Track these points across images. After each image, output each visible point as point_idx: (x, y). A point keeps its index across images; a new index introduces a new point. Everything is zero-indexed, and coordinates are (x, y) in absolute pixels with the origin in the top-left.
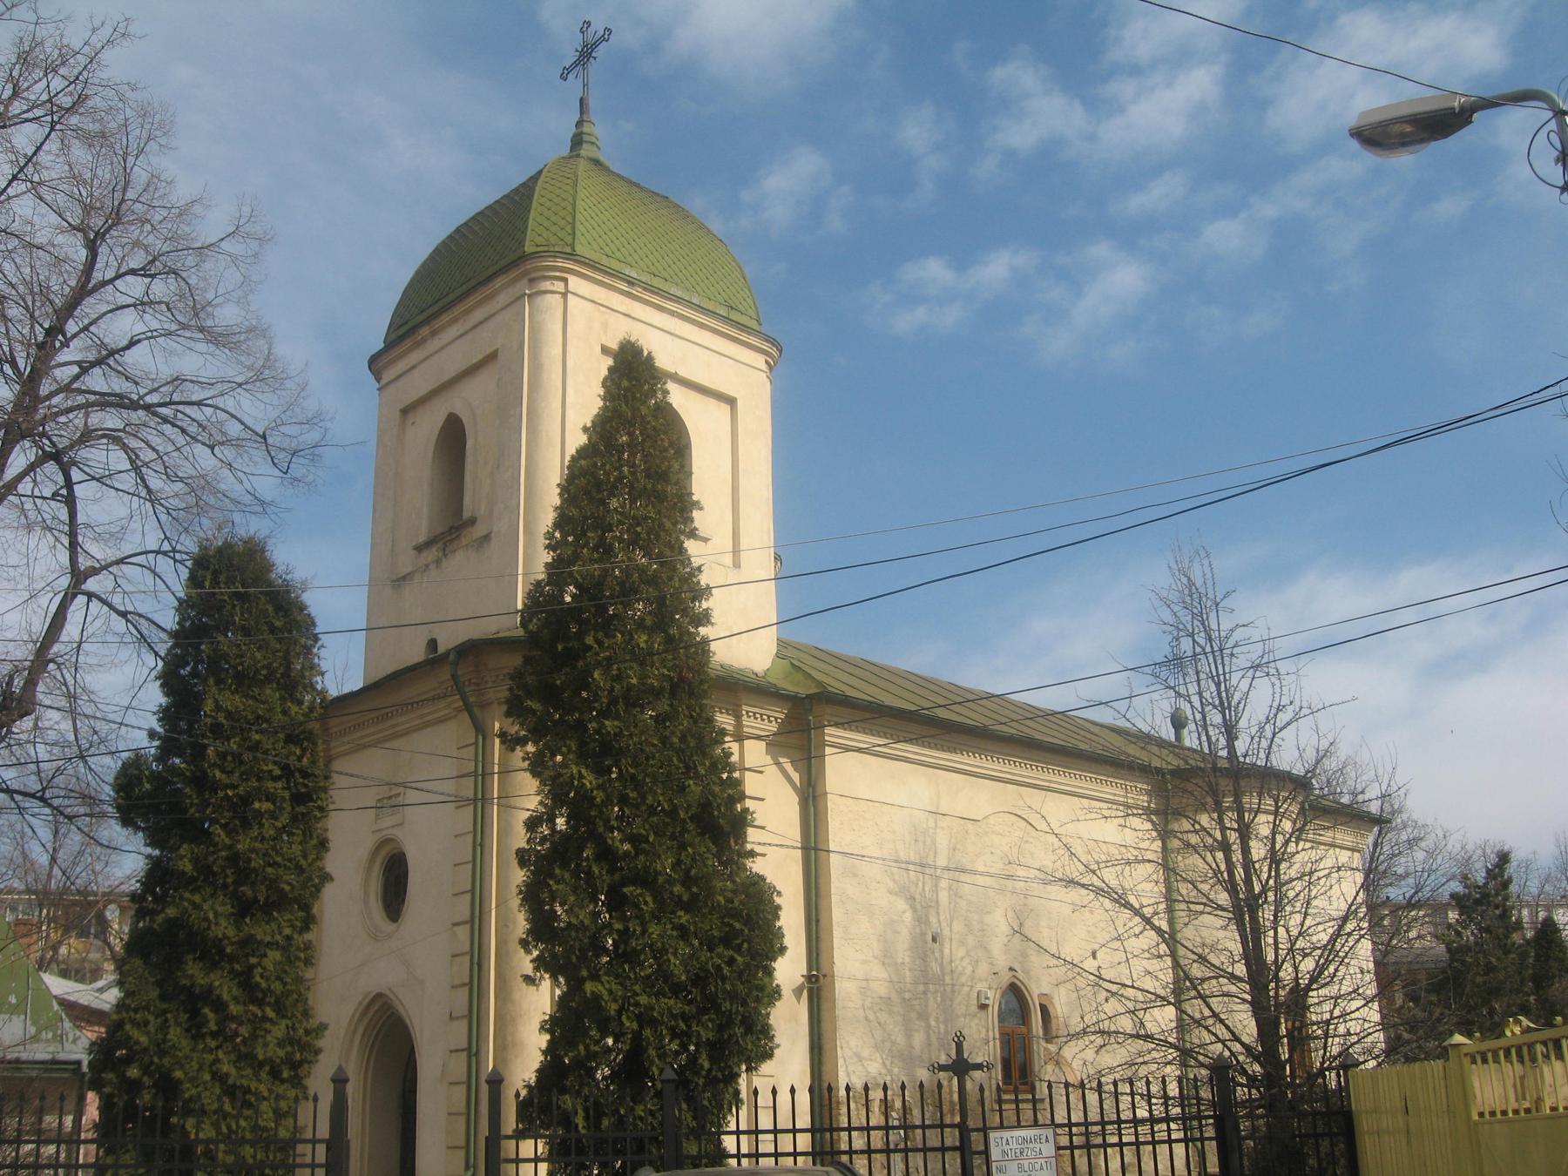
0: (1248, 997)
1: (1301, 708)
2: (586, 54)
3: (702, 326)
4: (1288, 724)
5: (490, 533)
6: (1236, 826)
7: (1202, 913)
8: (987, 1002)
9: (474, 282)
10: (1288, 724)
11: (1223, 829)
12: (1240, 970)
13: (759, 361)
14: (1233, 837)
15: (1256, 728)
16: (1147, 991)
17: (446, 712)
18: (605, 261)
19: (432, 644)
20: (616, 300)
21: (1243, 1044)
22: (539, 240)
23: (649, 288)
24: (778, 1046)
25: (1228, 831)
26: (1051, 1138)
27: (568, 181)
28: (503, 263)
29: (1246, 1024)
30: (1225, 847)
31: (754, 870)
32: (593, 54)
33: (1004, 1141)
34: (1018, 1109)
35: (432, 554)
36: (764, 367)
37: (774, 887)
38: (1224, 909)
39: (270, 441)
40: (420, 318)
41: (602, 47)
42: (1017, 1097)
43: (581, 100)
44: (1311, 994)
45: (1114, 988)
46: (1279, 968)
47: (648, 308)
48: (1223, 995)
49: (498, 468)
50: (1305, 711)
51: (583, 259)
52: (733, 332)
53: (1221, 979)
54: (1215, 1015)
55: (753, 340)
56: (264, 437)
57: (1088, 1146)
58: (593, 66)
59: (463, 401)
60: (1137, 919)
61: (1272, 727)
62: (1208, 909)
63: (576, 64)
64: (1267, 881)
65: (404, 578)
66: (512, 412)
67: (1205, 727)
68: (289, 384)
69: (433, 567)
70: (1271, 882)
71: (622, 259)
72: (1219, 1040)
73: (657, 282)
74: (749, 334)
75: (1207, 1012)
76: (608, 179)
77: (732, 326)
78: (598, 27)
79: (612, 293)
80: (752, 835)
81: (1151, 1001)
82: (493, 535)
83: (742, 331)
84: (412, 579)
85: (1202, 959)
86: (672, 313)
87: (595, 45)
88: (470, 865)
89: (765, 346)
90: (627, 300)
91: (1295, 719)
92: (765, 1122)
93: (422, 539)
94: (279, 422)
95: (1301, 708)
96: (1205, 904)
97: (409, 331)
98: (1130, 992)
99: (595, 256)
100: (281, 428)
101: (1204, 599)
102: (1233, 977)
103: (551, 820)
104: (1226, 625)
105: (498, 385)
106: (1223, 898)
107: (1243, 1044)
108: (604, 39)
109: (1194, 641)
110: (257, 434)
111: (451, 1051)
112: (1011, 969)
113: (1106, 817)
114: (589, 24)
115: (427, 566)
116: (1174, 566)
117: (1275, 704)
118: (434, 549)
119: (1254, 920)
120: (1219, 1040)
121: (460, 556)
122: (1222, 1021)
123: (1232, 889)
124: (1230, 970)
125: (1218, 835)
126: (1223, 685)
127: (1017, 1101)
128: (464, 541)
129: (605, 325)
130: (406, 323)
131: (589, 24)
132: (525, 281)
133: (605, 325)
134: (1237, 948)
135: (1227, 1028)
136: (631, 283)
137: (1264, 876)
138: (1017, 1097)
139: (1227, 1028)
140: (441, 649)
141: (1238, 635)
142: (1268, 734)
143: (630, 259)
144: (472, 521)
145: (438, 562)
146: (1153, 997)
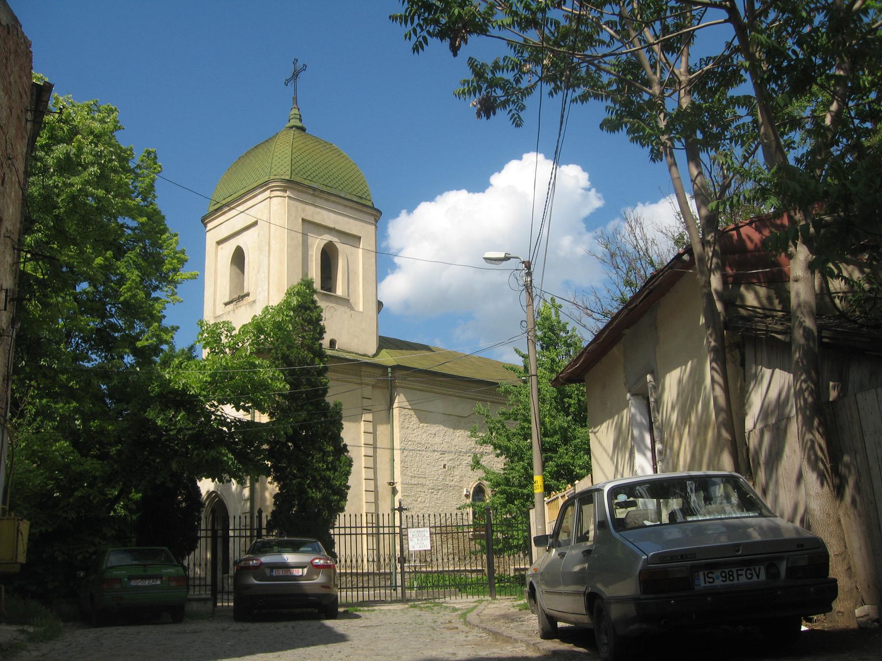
2: (295, 75)
3: (346, 206)
9: (247, 189)
22: (275, 173)
35: (231, 307)
40: (224, 202)
41: (303, 73)
43: (294, 98)
49: (259, 272)
52: (360, 207)
55: (369, 210)
59: (245, 241)
65: (219, 316)
69: (232, 312)
73: (324, 189)
76: (304, 141)
78: (300, 65)
87: (299, 72)
89: (374, 212)
93: (227, 300)
99: (298, 179)
115: (229, 312)
121: (243, 308)
129: (304, 210)
133: (304, 210)
143: (315, 180)
144: (248, 295)
145: (234, 310)
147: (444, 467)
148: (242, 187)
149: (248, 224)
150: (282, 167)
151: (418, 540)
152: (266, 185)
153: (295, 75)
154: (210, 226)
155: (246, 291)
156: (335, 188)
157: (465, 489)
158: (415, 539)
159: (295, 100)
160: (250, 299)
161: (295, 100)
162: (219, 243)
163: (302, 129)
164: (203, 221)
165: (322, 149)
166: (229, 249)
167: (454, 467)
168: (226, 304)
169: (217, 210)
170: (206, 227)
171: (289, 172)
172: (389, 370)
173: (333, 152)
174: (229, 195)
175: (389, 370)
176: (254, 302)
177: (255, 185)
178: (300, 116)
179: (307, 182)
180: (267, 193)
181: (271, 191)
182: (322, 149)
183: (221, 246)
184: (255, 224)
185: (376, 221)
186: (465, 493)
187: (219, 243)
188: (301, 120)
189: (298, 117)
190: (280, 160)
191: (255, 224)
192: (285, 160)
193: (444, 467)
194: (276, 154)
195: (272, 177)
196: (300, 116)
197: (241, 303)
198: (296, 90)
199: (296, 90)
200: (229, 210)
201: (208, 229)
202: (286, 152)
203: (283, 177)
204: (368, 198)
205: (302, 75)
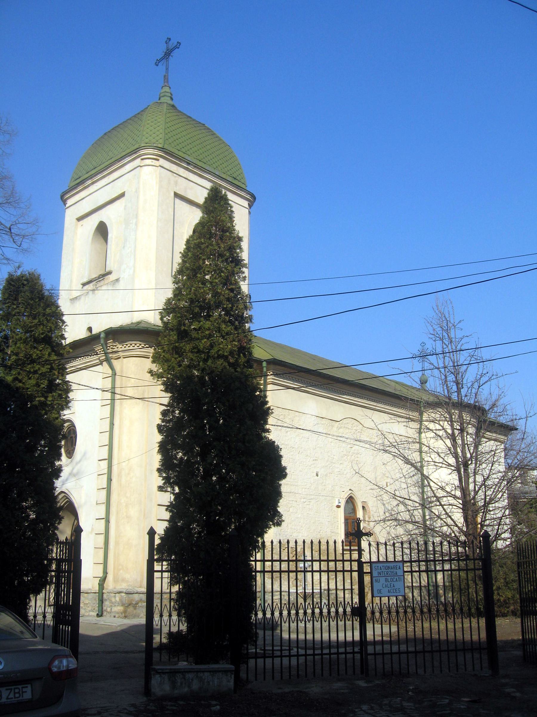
0: (461, 506)
1: (493, 375)
2: (168, 54)
4: (486, 382)
5: (119, 278)
6: (458, 427)
7: (441, 467)
8: (340, 504)
10: (486, 382)
11: (453, 429)
12: (458, 493)
13: (246, 204)
14: (456, 432)
15: (471, 384)
16: (416, 502)
17: (98, 361)
18: (177, 152)
19: (90, 329)
20: (182, 171)
21: (459, 528)
22: (147, 140)
23: (196, 166)
24: (284, 521)
25: (455, 430)
26: (401, 567)
27: (160, 113)
28: (128, 151)
29: (458, 517)
30: (453, 438)
31: (270, 439)
32: (171, 54)
33: (379, 568)
34: (351, 554)
35: (90, 287)
36: (247, 206)
37: (278, 446)
38: (452, 466)
39: (13, 231)
40: (87, 176)
42: (350, 548)
43: (165, 76)
44: (491, 505)
45: (401, 500)
46: (476, 493)
47: (196, 176)
48: (450, 505)
49: (124, 247)
50: (494, 377)
51: (167, 151)
53: (449, 498)
54: (447, 514)
55: (243, 194)
56: (10, 229)
57: (427, 571)
58: (172, 60)
60: (413, 469)
61: (478, 382)
62: (444, 466)
63: (162, 59)
64: (473, 453)
65: (76, 298)
66: (131, 222)
67: (446, 381)
68: (22, 205)
69: (91, 293)
70: (474, 454)
71: (184, 151)
72: (447, 525)
74: (241, 190)
75: (444, 512)
77: (234, 186)
79: (179, 168)
80: (271, 420)
81: (416, 507)
82: (120, 279)
83: (238, 189)
84: (80, 299)
85: (442, 488)
86: (206, 179)
88: (107, 434)
89: (248, 197)
90: (187, 172)
91: (490, 379)
92: (268, 557)
93: (85, 280)
94: (17, 222)
95: (493, 375)
96: (443, 463)
97: (81, 181)
98: (407, 502)
100: (18, 225)
101: (449, 323)
102: (455, 497)
103: (174, 412)
104: (459, 334)
105: (125, 209)
106: (452, 460)
107: (459, 528)
108: (176, 47)
109: (443, 341)
110: (6, 227)
111: (97, 519)
112: (350, 490)
113: (399, 422)
114: (170, 39)
116: (435, 308)
117: (480, 373)
118: (91, 285)
119: (466, 470)
120: (447, 525)
122: (450, 517)
123: (456, 457)
124: (453, 493)
125: (450, 431)
126: (456, 363)
127: (350, 550)
128: (106, 281)
129: (176, 183)
130: (80, 177)
131: (170, 39)
132: (139, 160)
133: (176, 183)
134: (457, 483)
135: (452, 519)
136: (188, 164)
137: (471, 451)
138: (350, 548)
139: (452, 519)
140: (94, 332)
141: (463, 341)
142: (476, 386)
143: (188, 152)
144: (110, 273)
146: (417, 505)
147: (317, 475)
148: (109, 157)
149: (113, 196)
150: (154, 135)
151: (386, 580)
152: (135, 153)
153: (168, 54)
154: (69, 202)
155: (108, 270)
156: (209, 165)
157: (337, 500)
158: (382, 580)
159: (166, 78)
160: (112, 277)
161: (166, 78)
162: (79, 219)
163: (173, 106)
164: (62, 197)
165: (195, 125)
166: (92, 222)
167: (326, 475)
168: (84, 285)
169: (78, 184)
170: (65, 204)
171: (161, 141)
172: (264, 364)
173: (207, 131)
174: (93, 167)
175: (264, 364)
176: (117, 280)
177: (124, 154)
178: (171, 94)
179: (180, 154)
180: (138, 162)
181: (142, 159)
182: (195, 125)
183: (81, 222)
184: (122, 195)
185: (250, 206)
186: (337, 504)
187: (79, 219)
188: (172, 99)
189: (169, 95)
190: (152, 128)
191: (122, 195)
192: (158, 128)
193: (317, 475)
194: (149, 122)
195: (143, 145)
196: (171, 94)
197: (102, 283)
198: (167, 69)
199: (167, 69)
200: (93, 183)
201: (67, 206)
202: (159, 120)
203: (155, 145)
204: (242, 181)
205: (176, 53)
